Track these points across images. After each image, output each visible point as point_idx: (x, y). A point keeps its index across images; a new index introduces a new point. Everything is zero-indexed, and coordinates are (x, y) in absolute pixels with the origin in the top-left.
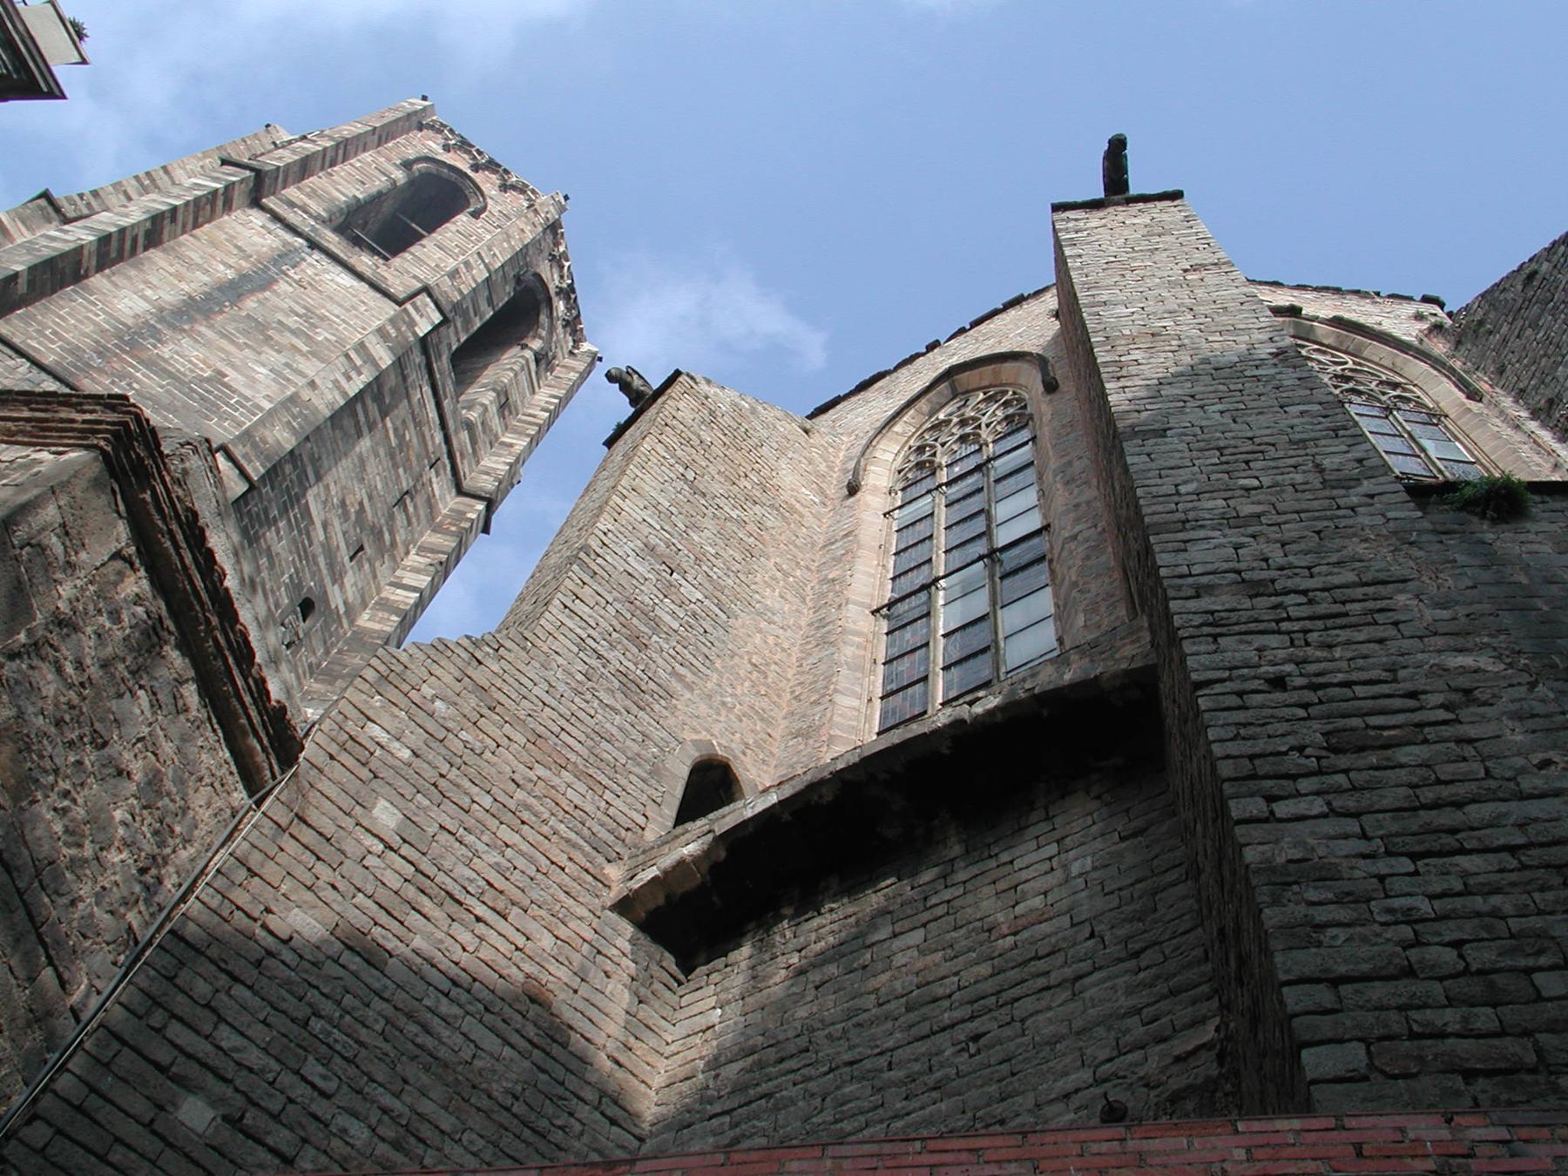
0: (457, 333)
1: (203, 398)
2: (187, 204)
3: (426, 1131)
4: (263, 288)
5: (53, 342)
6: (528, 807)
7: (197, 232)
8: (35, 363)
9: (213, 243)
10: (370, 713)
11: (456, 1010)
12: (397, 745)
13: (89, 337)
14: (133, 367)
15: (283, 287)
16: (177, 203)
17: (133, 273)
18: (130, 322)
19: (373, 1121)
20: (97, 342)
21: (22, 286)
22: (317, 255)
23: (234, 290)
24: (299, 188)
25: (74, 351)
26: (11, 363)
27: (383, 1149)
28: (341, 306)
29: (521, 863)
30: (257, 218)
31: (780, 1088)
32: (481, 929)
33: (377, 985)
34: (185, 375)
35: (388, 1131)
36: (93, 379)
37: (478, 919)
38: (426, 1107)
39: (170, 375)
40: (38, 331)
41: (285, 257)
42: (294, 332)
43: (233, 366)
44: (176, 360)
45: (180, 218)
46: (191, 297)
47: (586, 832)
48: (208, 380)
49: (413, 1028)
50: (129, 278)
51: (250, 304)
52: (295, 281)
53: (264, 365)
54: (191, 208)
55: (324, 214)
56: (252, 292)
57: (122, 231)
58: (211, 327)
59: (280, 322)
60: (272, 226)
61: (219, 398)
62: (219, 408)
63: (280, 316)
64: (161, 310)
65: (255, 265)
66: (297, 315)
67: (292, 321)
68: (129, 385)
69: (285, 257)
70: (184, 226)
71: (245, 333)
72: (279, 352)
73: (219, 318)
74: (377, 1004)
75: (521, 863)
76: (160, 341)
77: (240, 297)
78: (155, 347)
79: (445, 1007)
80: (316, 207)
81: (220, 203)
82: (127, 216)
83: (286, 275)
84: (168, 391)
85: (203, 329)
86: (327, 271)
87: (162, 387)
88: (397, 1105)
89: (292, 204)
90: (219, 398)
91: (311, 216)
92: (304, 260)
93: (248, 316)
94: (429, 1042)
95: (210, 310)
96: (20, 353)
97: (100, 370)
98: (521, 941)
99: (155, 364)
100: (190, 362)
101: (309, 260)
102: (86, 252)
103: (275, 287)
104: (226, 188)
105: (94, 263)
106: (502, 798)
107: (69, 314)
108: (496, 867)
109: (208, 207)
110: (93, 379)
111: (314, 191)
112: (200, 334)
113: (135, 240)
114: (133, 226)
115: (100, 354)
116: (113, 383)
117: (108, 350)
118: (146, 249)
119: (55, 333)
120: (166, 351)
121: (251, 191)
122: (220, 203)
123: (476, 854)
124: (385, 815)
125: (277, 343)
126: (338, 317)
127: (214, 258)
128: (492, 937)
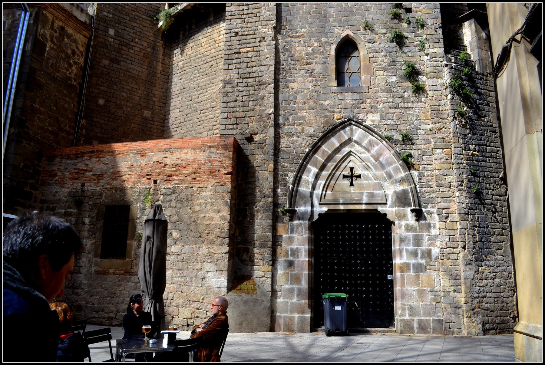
3: (134, 90)
6: (136, 15)
10: (102, 10)
11: (133, 66)
12: (109, 14)
19: (126, 91)
27: (129, 95)
29: (138, 29)
31: (187, 69)
32: (134, 48)
33: (120, 68)
35: (128, 92)
37: (133, 46)
38: (133, 86)
47: (148, 15)
49: (127, 73)
74: (121, 71)
75: (138, 29)
79: (132, 66)
88: (129, 87)
94: (131, 74)
98: (141, 47)
106: (131, 16)
108: (134, 33)
123: (129, 32)
124: (112, 32)
128: (136, 49)
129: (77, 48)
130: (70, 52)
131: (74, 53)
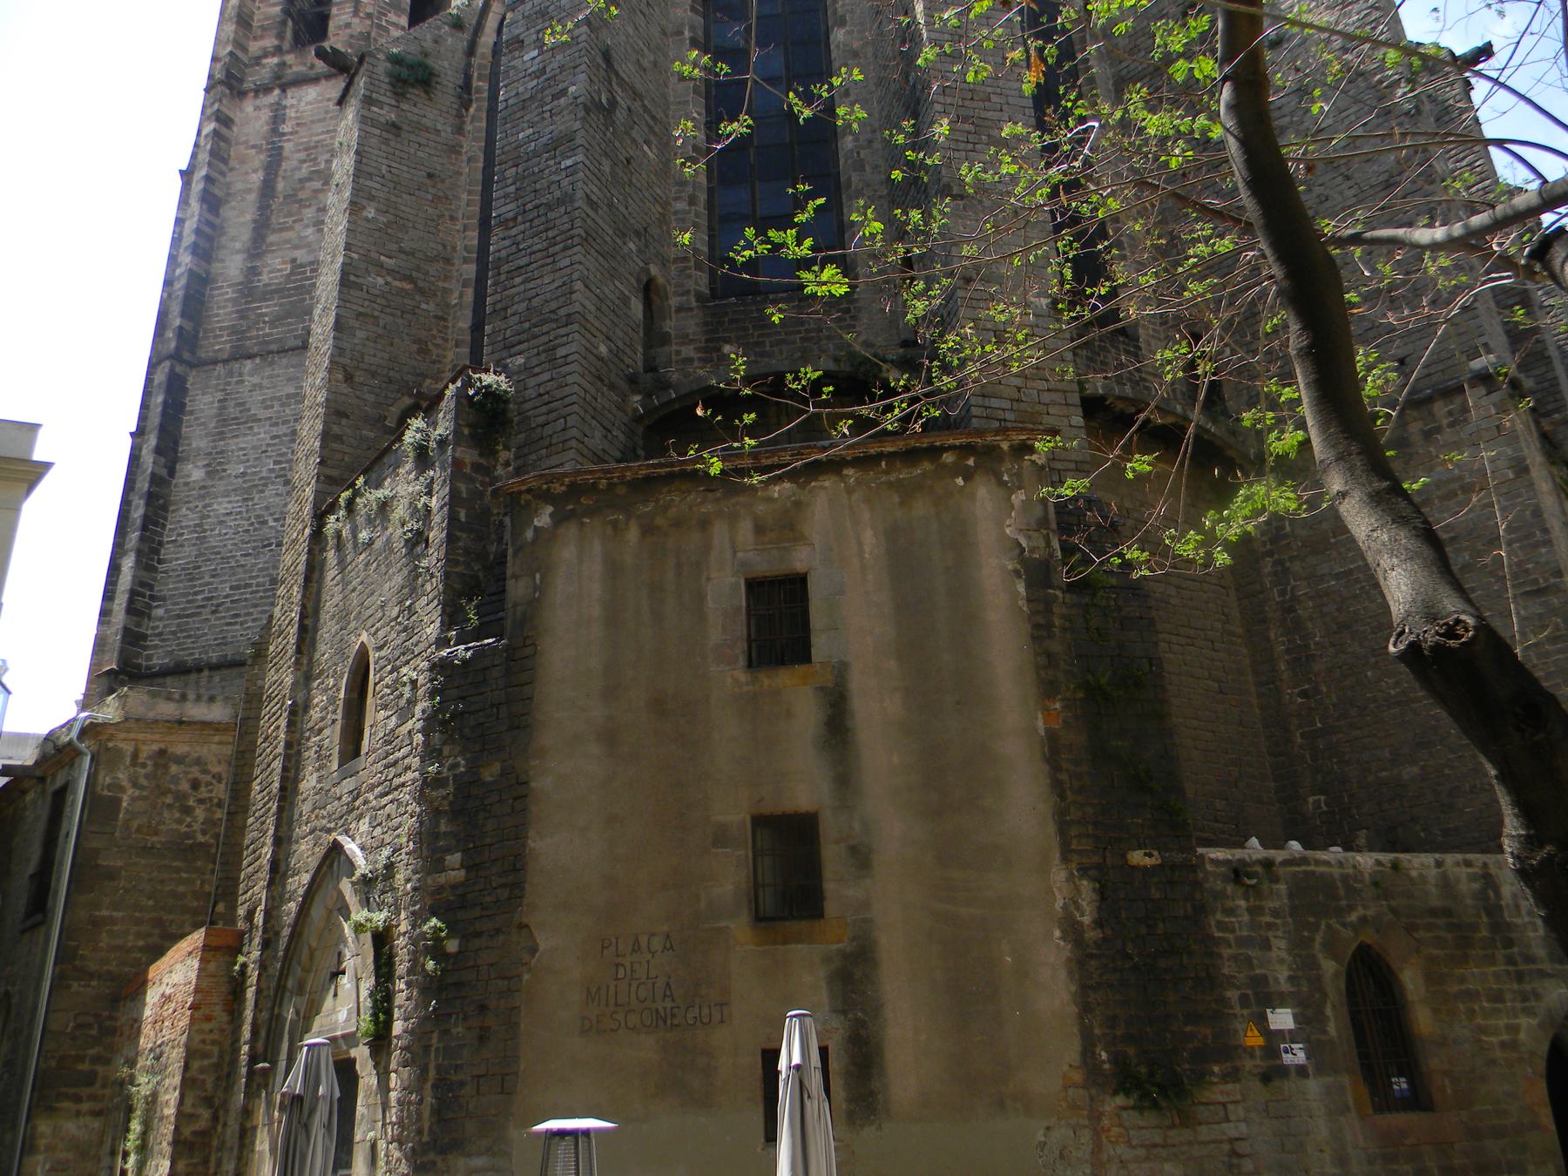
0: (395, 25)
1: (295, 288)
2: (210, 164)
4: (279, 165)
5: (222, 336)
7: (232, 163)
8: (225, 361)
9: (243, 161)
13: (232, 312)
14: (259, 308)
15: (288, 147)
16: (203, 172)
17: (224, 239)
18: (241, 279)
20: (237, 312)
21: (188, 326)
22: (289, 93)
23: (267, 189)
24: (255, 39)
25: (234, 331)
26: (216, 373)
28: (320, 121)
30: (249, 106)
34: (280, 283)
36: (250, 339)
39: (276, 291)
40: (216, 337)
41: (278, 116)
42: (309, 179)
43: (296, 247)
44: (271, 279)
45: (215, 175)
46: (255, 221)
48: (292, 273)
50: (224, 247)
51: (280, 186)
52: (291, 133)
53: (307, 226)
54: (215, 162)
55: (276, 42)
56: (276, 175)
57: (198, 232)
58: (274, 231)
59: (301, 181)
60: (258, 102)
61: (301, 280)
62: (304, 286)
63: (298, 175)
64: (248, 250)
65: (268, 150)
66: (304, 161)
67: (304, 171)
68: (264, 322)
69: (278, 116)
70: (223, 174)
71: (289, 215)
72: (309, 206)
73: (273, 220)
76: (260, 274)
77: (273, 188)
78: (259, 281)
80: (270, 42)
81: (224, 131)
82: (193, 216)
83: (284, 134)
84: (281, 305)
85: (272, 238)
86: (300, 100)
87: (275, 305)
89: (257, 61)
90: (301, 280)
91: (273, 55)
92: (285, 107)
93: (285, 197)
95: (268, 219)
96: (215, 362)
97: (249, 328)
99: (265, 293)
100: (279, 270)
101: (288, 102)
102: (195, 268)
103: (286, 153)
104: (218, 120)
105: (203, 263)
107: (219, 308)
109: (222, 144)
110: (250, 339)
111: (263, 28)
112: (272, 244)
113: (209, 224)
114: (199, 221)
115: (242, 318)
116: (258, 330)
117: (242, 310)
118: (217, 215)
119: (221, 329)
120: (265, 278)
121: (231, 94)
122: (224, 131)
125: (307, 199)
126: (323, 133)
127: (247, 173)
129: (205, 772)
130: (185, 786)
131: (195, 785)
